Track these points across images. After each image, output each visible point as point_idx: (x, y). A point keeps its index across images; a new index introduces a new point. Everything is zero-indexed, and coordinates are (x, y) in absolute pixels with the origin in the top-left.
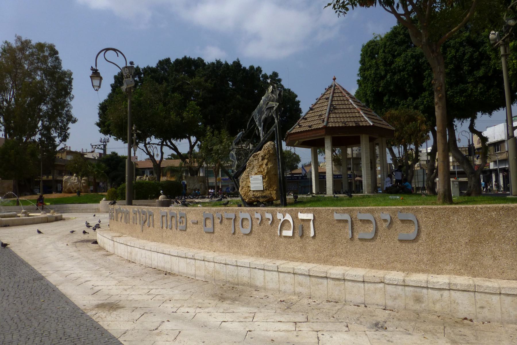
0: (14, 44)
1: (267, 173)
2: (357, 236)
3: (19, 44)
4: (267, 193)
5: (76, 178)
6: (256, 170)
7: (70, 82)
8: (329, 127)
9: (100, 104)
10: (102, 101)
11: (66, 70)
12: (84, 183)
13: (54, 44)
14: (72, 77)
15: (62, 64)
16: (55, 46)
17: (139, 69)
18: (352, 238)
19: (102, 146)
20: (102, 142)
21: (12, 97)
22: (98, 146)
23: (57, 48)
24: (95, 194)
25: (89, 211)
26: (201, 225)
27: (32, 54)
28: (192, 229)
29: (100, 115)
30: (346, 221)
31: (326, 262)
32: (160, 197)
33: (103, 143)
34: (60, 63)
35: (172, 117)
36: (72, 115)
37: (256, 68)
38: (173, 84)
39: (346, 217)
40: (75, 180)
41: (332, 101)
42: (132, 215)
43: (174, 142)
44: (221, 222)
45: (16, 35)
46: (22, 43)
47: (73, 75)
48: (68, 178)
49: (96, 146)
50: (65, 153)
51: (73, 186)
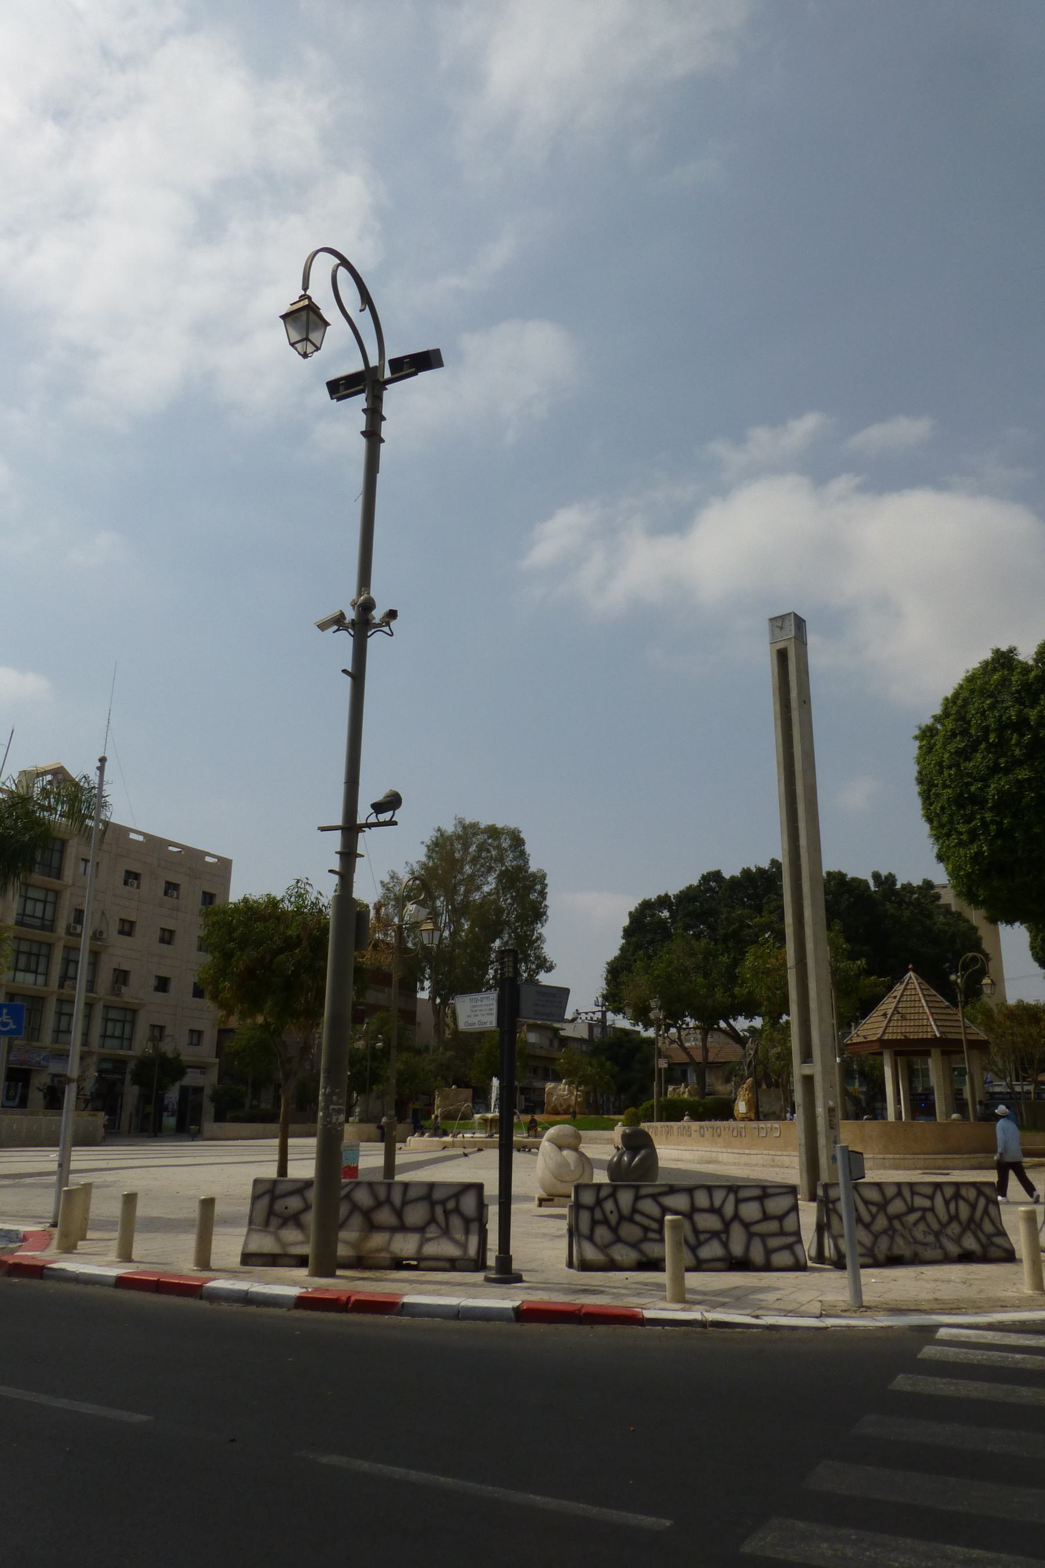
0: (450, 828)
1: (748, 1101)
2: (761, 1135)
3: (460, 830)
7: (543, 894)
8: (884, 1040)
9: (608, 964)
11: (535, 870)
13: (520, 829)
14: (546, 882)
16: (521, 832)
17: (670, 897)
18: (759, 1136)
19: (599, 1015)
20: (598, 1006)
21: (444, 926)
22: (592, 1015)
23: (522, 835)
24: (598, 1116)
26: (698, 1133)
27: (481, 848)
28: (695, 1135)
29: (608, 983)
32: (685, 1118)
33: (600, 1008)
34: (527, 862)
36: (547, 957)
37: (886, 878)
38: (724, 929)
39: (756, 1126)
40: (564, 1091)
41: (899, 1002)
43: (731, 1021)
44: (707, 1130)
45: (456, 816)
46: (464, 827)
47: (547, 878)
48: (553, 1088)
49: (587, 1013)
50: (525, 1028)
51: (562, 1101)
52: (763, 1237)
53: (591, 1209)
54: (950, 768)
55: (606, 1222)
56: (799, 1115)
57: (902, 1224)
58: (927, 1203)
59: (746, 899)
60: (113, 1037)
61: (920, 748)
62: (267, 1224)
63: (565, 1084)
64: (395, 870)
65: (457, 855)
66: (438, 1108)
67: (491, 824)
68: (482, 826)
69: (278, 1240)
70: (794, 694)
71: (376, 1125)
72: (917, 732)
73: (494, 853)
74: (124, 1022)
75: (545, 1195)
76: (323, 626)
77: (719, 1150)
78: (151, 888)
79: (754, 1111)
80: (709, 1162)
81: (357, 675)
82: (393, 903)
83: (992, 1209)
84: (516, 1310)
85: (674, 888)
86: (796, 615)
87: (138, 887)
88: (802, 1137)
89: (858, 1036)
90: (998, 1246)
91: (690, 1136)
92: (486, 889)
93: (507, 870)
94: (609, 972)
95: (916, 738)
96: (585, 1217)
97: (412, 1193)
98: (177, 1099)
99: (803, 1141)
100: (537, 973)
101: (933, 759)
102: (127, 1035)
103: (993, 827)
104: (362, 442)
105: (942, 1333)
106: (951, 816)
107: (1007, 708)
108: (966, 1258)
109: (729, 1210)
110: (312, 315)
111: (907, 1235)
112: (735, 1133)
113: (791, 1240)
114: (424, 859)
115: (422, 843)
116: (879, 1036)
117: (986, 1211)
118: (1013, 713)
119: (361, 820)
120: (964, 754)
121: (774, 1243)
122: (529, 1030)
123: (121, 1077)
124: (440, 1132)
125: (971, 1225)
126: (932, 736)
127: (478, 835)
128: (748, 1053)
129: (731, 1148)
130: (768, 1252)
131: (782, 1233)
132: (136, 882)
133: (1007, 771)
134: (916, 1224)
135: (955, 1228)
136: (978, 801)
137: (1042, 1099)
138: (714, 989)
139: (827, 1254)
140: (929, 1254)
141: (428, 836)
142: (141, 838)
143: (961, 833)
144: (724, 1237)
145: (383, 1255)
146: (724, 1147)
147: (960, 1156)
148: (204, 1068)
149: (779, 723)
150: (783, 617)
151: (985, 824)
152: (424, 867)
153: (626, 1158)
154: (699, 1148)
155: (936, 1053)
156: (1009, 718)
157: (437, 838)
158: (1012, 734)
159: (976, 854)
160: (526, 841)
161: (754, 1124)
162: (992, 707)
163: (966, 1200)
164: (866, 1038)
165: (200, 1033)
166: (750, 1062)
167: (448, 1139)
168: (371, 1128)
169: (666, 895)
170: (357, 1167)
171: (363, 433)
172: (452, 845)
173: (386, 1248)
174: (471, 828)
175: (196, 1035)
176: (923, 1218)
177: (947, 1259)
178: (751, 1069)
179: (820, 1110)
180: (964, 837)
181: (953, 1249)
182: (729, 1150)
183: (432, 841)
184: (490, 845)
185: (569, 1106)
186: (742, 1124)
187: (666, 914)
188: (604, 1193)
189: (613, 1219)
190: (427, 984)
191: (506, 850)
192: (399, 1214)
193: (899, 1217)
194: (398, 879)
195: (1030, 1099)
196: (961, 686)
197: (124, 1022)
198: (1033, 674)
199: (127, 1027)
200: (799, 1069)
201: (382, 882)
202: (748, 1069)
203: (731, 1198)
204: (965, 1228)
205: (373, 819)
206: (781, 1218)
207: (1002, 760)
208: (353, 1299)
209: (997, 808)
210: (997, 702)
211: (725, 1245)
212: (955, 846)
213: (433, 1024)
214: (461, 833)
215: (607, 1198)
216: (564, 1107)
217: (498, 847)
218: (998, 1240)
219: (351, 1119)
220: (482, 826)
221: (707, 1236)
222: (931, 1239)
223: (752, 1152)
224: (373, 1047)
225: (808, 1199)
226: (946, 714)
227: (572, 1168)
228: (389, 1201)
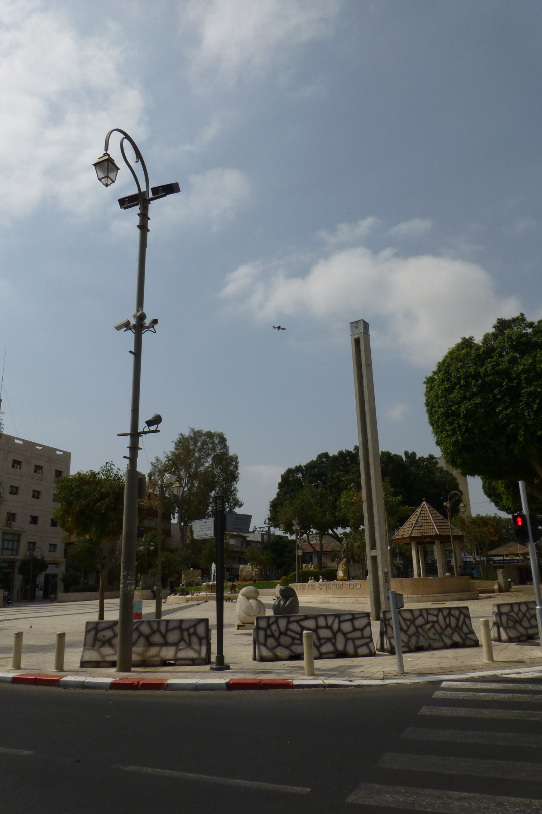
0: (187, 434)
1: (344, 570)
3: (192, 435)
4: (344, 577)
5: (251, 566)
6: (341, 569)
7: (236, 467)
9: (271, 502)
10: (272, 499)
12: (257, 571)
14: (238, 461)
15: (229, 450)
16: (224, 435)
17: (302, 467)
18: (350, 588)
19: (266, 529)
20: (266, 524)
21: (185, 485)
22: (263, 529)
23: (225, 436)
24: (267, 581)
25: (268, 594)
26: (319, 588)
27: (204, 443)
28: (317, 589)
29: (271, 512)
30: (348, 584)
31: (345, 595)
33: (267, 525)
34: (227, 450)
35: (327, 517)
36: (239, 500)
37: (412, 454)
38: (330, 482)
40: (249, 569)
41: (419, 517)
42: (299, 587)
43: (335, 530)
45: (190, 427)
46: (194, 433)
47: (238, 458)
48: (244, 567)
49: (260, 528)
50: (228, 537)
52: (353, 640)
53: (265, 630)
54: (442, 398)
55: (272, 636)
56: (370, 577)
57: (423, 631)
58: (435, 619)
59: (341, 467)
60: (8, 549)
61: (427, 388)
62: (94, 645)
63: (250, 565)
64: (159, 456)
65: (191, 448)
66: (183, 581)
67: (208, 430)
68: (204, 432)
69: (100, 654)
70: (363, 362)
71: (151, 590)
72: (425, 380)
73: (210, 446)
74: (13, 541)
75: (241, 624)
76: (118, 328)
77: (329, 596)
78: (27, 469)
79: (347, 576)
80: (325, 603)
81: (137, 354)
82: (157, 473)
83: (467, 621)
84: (227, 684)
85: (304, 462)
86: (363, 321)
87: (20, 468)
88: (372, 588)
89: (399, 535)
90: (471, 639)
91: (315, 590)
92: (207, 465)
93: (217, 455)
94: (271, 506)
95: (425, 383)
96: (262, 633)
97: (171, 626)
98: (43, 581)
99: (372, 590)
100: (234, 508)
101: (433, 393)
102: (15, 547)
103: (463, 428)
104: (138, 231)
105: (444, 684)
106: (443, 422)
107: (469, 367)
108: (455, 645)
109: (335, 627)
110: (110, 164)
111: (426, 635)
112: (338, 587)
113: (367, 640)
114: (173, 450)
115: (173, 441)
116: (409, 535)
117: (464, 622)
118: (472, 370)
119: (140, 430)
120: (449, 391)
121: (358, 643)
122: (230, 538)
123: (12, 570)
124: (185, 593)
125: (457, 629)
126: (432, 382)
127: (202, 436)
128: (343, 546)
129: (336, 595)
130: (356, 647)
131: (363, 637)
132: (18, 466)
133: (470, 399)
134: (429, 629)
135: (449, 631)
136: (456, 414)
137: (489, 564)
138: (325, 513)
139: (385, 647)
140: (437, 644)
141: (176, 438)
142: (21, 442)
143: (447, 431)
144: (333, 641)
145: (157, 659)
146: (332, 595)
147: (450, 594)
148: (58, 564)
149: (356, 376)
150: (357, 322)
151: (459, 426)
152: (174, 454)
153: (282, 602)
154: (319, 596)
155: (437, 542)
156: (470, 372)
157: (180, 439)
158: (472, 380)
159: (455, 441)
160: (227, 440)
161: (347, 582)
162: (462, 367)
163: (454, 616)
164: (402, 536)
165: (55, 545)
166: (345, 550)
167: (189, 596)
168: (148, 592)
169: (300, 466)
170: (141, 613)
171: (138, 226)
172: (188, 442)
173: (158, 655)
174: (198, 433)
175: (53, 547)
176: (433, 626)
177: (446, 647)
178: (345, 554)
179: (380, 574)
180: (449, 433)
181: (448, 641)
182: (335, 596)
183: (178, 440)
184: (207, 442)
185: (252, 576)
186: (341, 583)
187: (300, 475)
188: (271, 621)
189: (276, 634)
190: (176, 515)
191: (217, 444)
192: (164, 636)
193: (421, 626)
194: (160, 460)
195: (484, 564)
196: (447, 356)
197: (13, 541)
198: (482, 350)
199: (15, 543)
200: (369, 553)
201: (151, 463)
202: (344, 554)
203: (337, 620)
204: (454, 631)
205: (147, 429)
206: (362, 630)
207: (467, 394)
208: (141, 683)
209: (465, 418)
210: (464, 364)
211: (334, 645)
212: (445, 437)
213: (180, 536)
214: (193, 436)
215: (273, 623)
216: (249, 577)
217: (213, 443)
218: (470, 636)
219: (137, 588)
220: (204, 432)
221: (325, 641)
222: (437, 637)
223: (347, 596)
224: (149, 550)
225: (375, 619)
226: (439, 370)
227: (255, 608)
228: (159, 630)
